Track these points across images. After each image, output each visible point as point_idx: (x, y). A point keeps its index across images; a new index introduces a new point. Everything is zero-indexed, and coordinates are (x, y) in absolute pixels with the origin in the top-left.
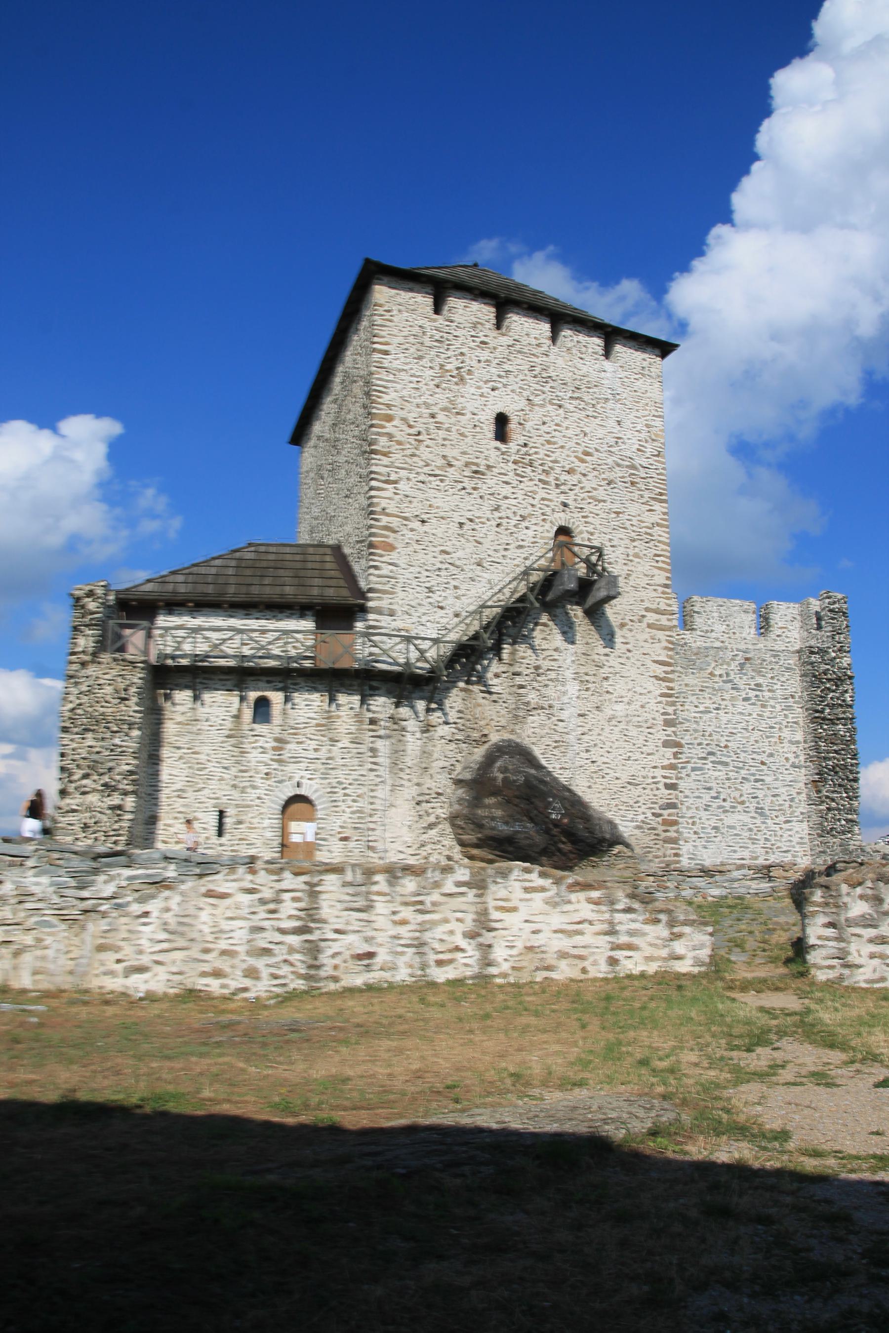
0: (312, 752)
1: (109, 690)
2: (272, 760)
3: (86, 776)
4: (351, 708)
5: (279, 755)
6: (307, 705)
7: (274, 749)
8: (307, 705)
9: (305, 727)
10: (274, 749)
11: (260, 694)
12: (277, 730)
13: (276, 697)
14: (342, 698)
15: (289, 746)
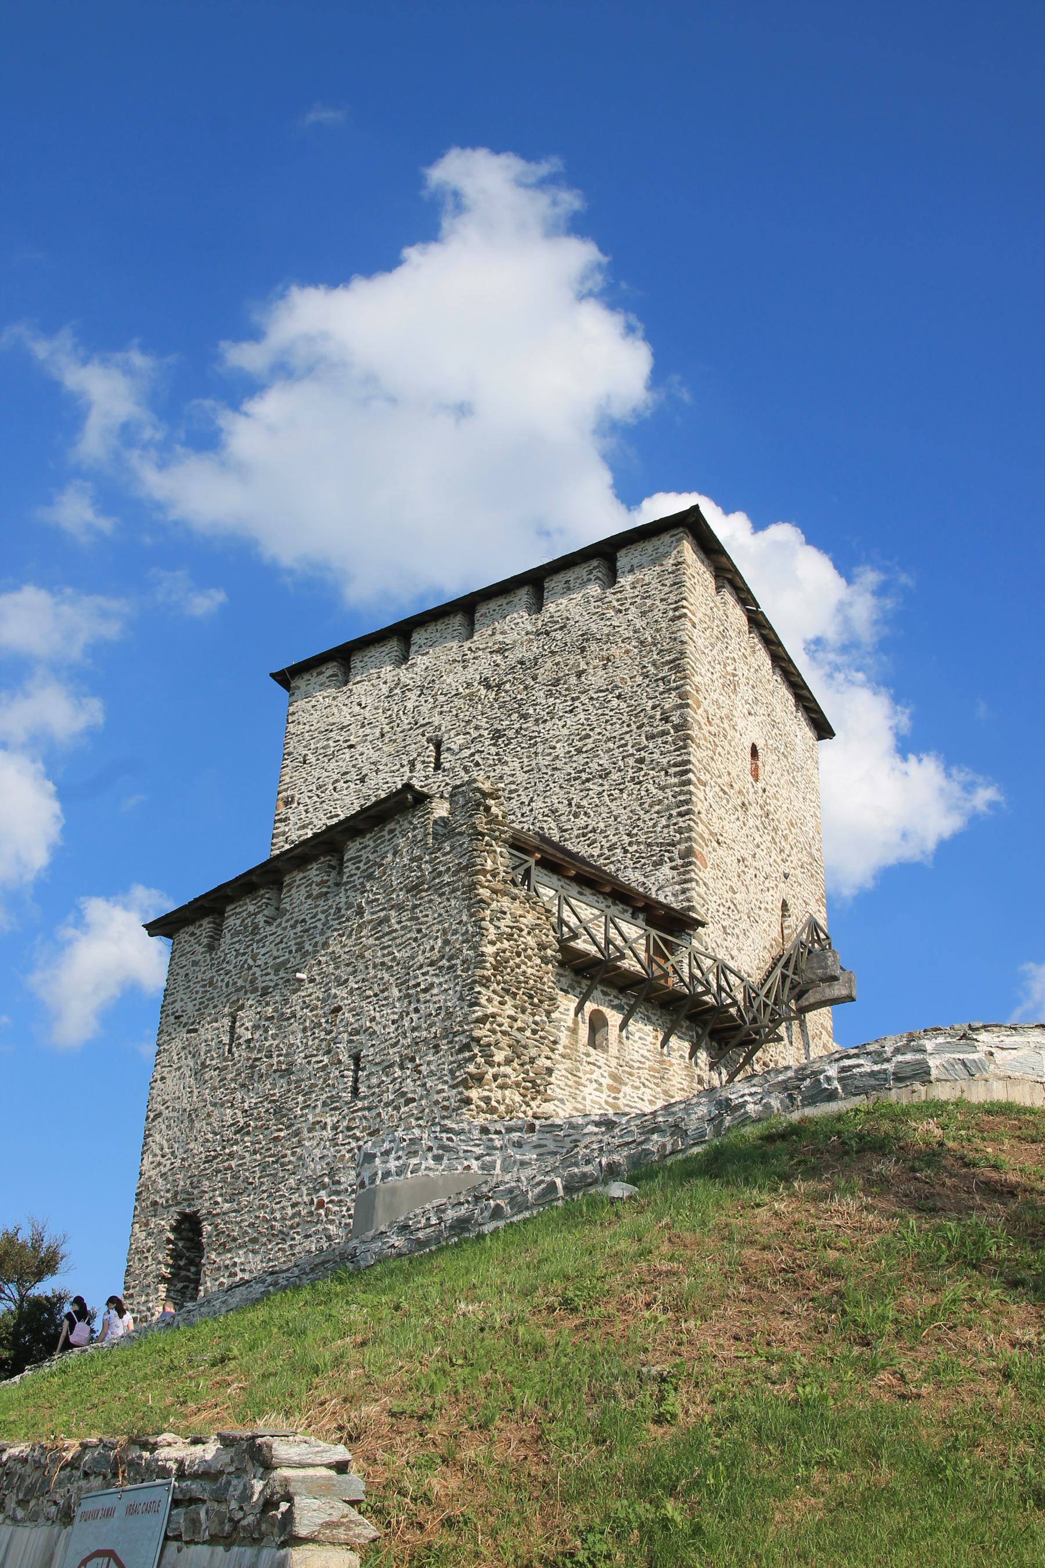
0: (647, 1103)
1: (531, 941)
2: (606, 1102)
3: (508, 1062)
4: (682, 1056)
5: (615, 1098)
6: (640, 1038)
7: (610, 1088)
8: (640, 1038)
9: (639, 1068)
10: (610, 1088)
11: (595, 1006)
12: (614, 1062)
13: (614, 1018)
14: (674, 1041)
15: (624, 1089)
